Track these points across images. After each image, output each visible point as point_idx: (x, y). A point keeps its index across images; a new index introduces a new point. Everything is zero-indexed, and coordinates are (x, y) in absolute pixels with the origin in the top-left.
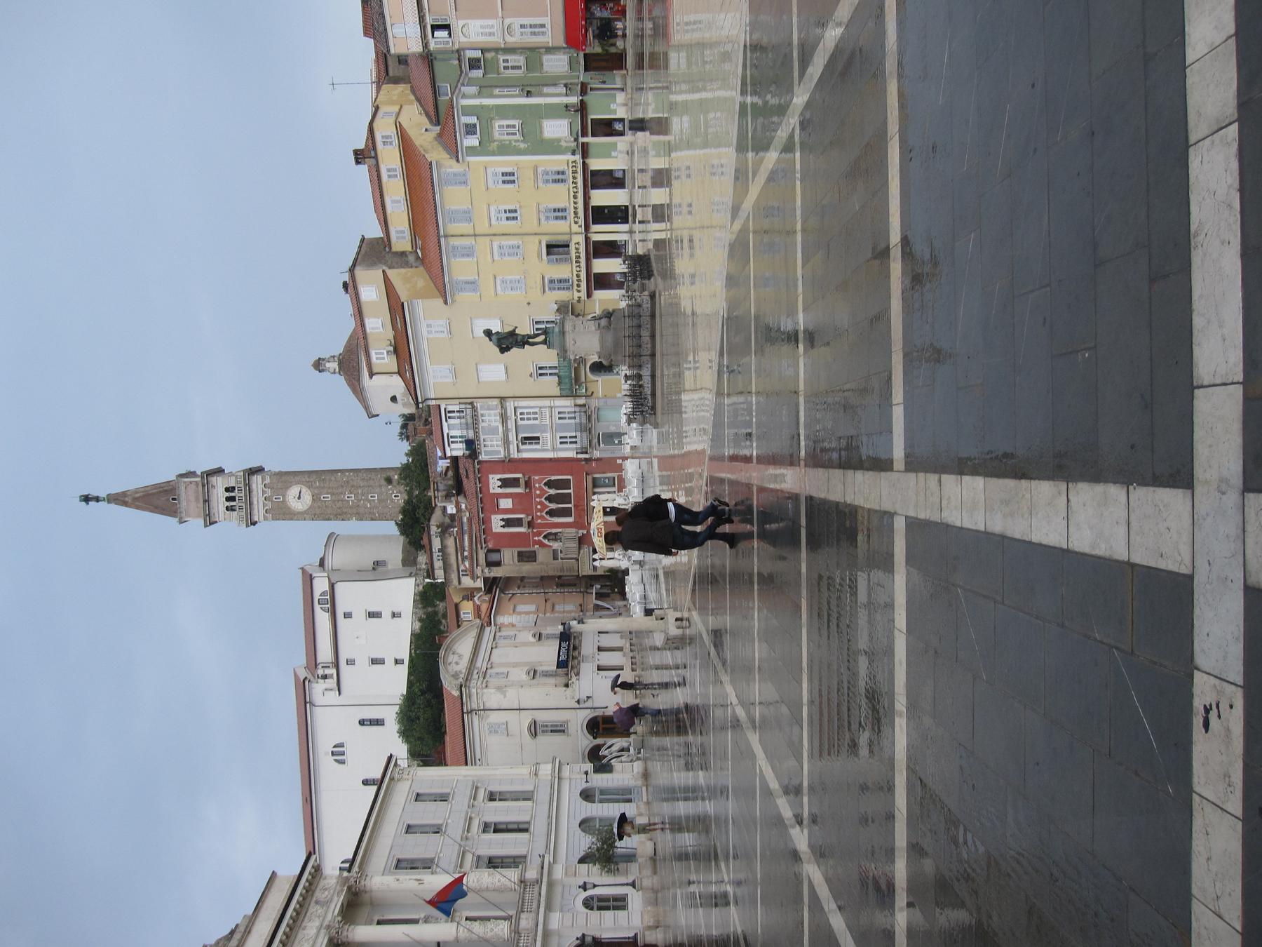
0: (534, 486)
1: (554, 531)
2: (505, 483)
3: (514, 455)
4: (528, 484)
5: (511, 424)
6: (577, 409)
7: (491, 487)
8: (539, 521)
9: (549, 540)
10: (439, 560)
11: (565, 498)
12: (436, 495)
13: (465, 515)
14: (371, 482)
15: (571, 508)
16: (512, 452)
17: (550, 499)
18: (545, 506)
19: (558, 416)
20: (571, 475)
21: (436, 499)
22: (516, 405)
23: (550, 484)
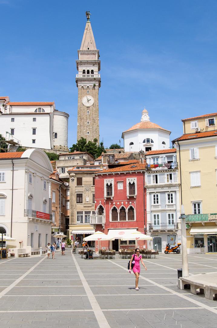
0: (130, 201)
1: (104, 211)
2: (132, 186)
3: (148, 191)
4: (132, 198)
5: (166, 189)
6: (176, 224)
7: (130, 179)
8: (110, 203)
9: (99, 208)
10: (69, 158)
11: (123, 217)
12: (107, 156)
13: (101, 168)
14: (95, 133)
15: (117, 220)
16: (149, 189)
17: (123, 209)
18: (119, 206)
19: (171, 214)
20: (136, 221)
21: (105, 156)
22: (177, 192)
23: (131, 209)
